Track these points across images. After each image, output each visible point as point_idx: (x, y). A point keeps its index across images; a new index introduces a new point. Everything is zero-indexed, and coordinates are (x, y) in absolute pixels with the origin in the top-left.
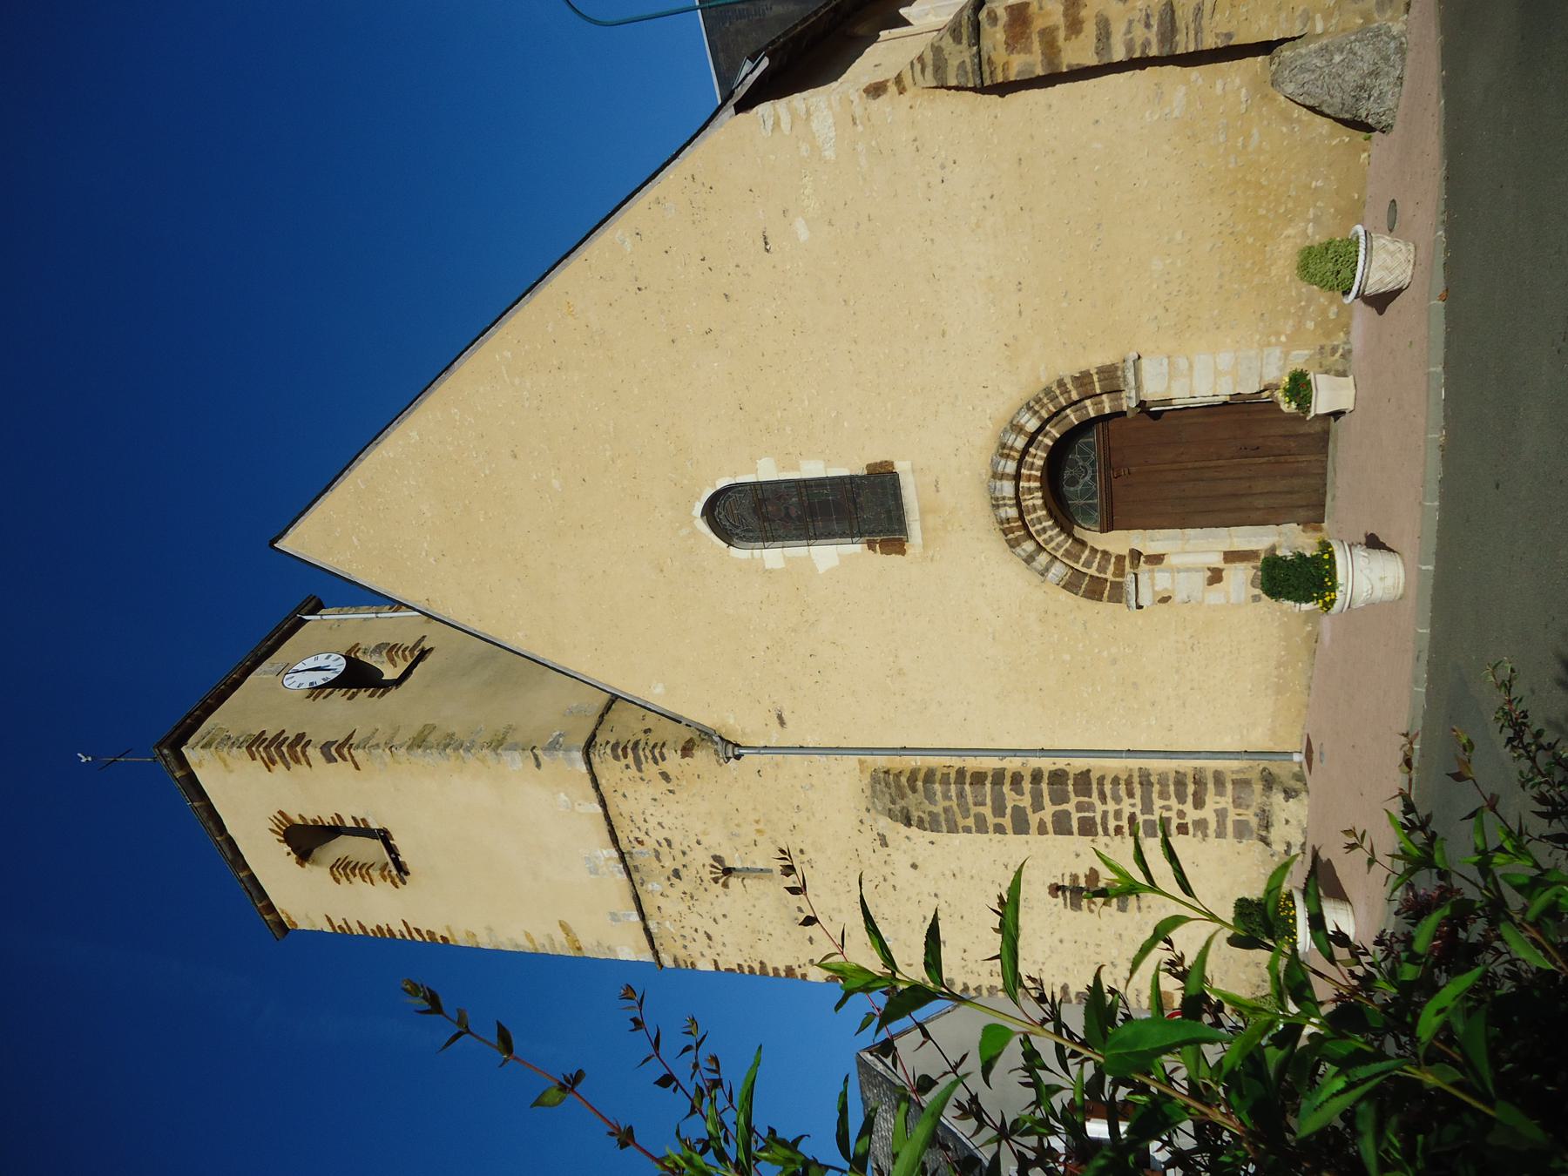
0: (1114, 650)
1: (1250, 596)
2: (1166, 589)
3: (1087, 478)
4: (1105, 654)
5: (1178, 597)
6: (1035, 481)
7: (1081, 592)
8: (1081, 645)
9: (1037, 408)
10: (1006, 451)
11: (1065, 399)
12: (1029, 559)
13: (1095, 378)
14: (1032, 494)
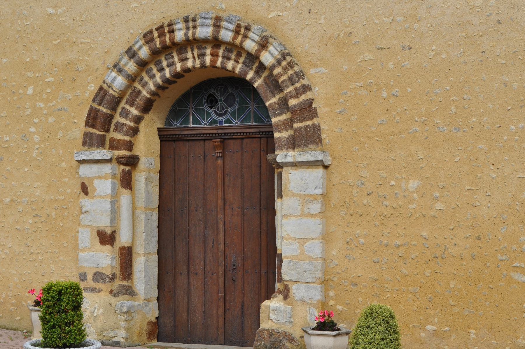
0: (36, 138)
1: (86, 270)
2: (95, 190)
3: (214, 116)
4: (33, 129)
5: (86, 202)
6: (211, 61)
7: (96, 106)
8: (42, 105)
9: (284, 63)
10: (242, 31)
11: (290, 92)
12: (131, 53)
13: (309, 123)
14: (199, 58)
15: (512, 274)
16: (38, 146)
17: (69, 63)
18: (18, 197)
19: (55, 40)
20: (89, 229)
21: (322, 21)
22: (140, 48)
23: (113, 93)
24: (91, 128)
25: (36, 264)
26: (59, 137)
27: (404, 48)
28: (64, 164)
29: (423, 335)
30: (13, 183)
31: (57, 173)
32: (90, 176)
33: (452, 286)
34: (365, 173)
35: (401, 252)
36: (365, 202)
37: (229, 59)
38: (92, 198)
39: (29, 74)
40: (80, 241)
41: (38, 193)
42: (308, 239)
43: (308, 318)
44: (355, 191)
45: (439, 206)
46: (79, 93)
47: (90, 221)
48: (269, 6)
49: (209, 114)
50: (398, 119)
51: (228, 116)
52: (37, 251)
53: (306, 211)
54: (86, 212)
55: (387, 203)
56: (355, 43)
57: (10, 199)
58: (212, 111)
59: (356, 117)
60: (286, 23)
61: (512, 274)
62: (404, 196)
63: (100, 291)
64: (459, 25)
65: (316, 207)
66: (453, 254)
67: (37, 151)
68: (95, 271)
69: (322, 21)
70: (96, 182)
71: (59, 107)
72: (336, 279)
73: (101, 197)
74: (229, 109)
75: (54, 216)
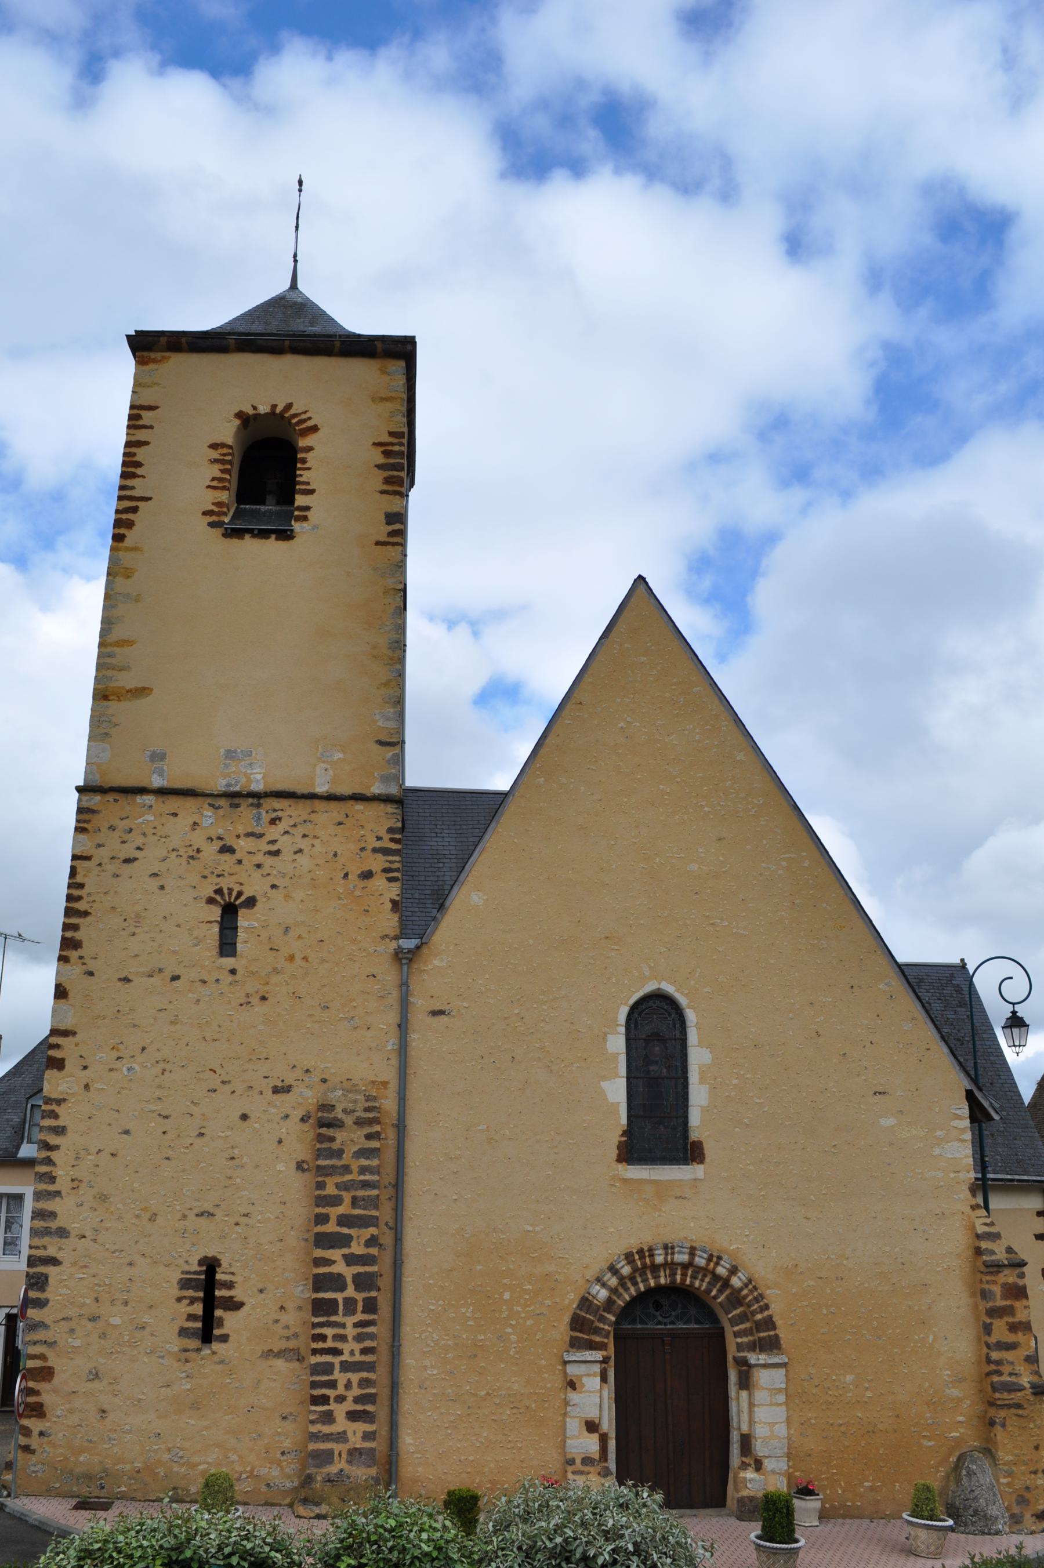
0: (513, 1338)
1: (574, 1456)
2: (583, 1386)
3: (660, 1318)
4: (509, 1330)
5: (573, 1396)
6: (681, 1279)
7: (578, 1312)
8: (519, 1309)
9: (750, 1287)
10: (715, 1259)
11: (756, 1309)
12: (613, 1270)
13: (772, 1333)
14: (669, 1276)
15: (922, 1441)
16: (515, 1345)
17: (547, 1275)
18: (494, 1390)
19: (533, 1254)
20: (577, 1420)
21: (774, 1254)
22: (623, 1267)
23: (599, 1304)
24: (210, 1256)
25: (515, 1451)
26: (537, 1338)
27: (837, 1278)
28: (543, 1361)
29: (862, 1490)
30: (489, 1378)
31: (536, 1370)
32: (579, 1373)
33: (881, 1452)
34: (813, 1371)
35: (843, 1429)
36: (814, 1392)
37: (696, 1278)
38: (581, 1393)
39: (505, 1281)
40: (568, 1430)
41: (516, 1387)
42: (777, 1423)
43: (778, 1485)
44: (805, 1384)
45: (869, 1394)
46: (558, 1300)
47: (579, 1413)
48: (731, 1240)
49: (655, 1317)
50: (835, 1330)
51: (672, 1318)
52: (515, 1440)
53: (774, 1401)
54: (574, 1405)
55: (830, 1393)
56: (801, 1273)
57: (485, 1392)
58: (658, 1314)
59: (804, 1328)
60: (745, 1254)
61: (922, 1441)
62: (844, 1387)
63: (588, 1473)
64: (876, 1264)
65: (782, 1398)
66: (881, 1429)
67: (514, 1350)
68: (584, 1456)
69: (774, 1254)
70: (585, 1380)
71: (538, 1312)
72: (793, 1452)
73: (590, 1392)
74: (673, 1313)
75: (534, 1408)
